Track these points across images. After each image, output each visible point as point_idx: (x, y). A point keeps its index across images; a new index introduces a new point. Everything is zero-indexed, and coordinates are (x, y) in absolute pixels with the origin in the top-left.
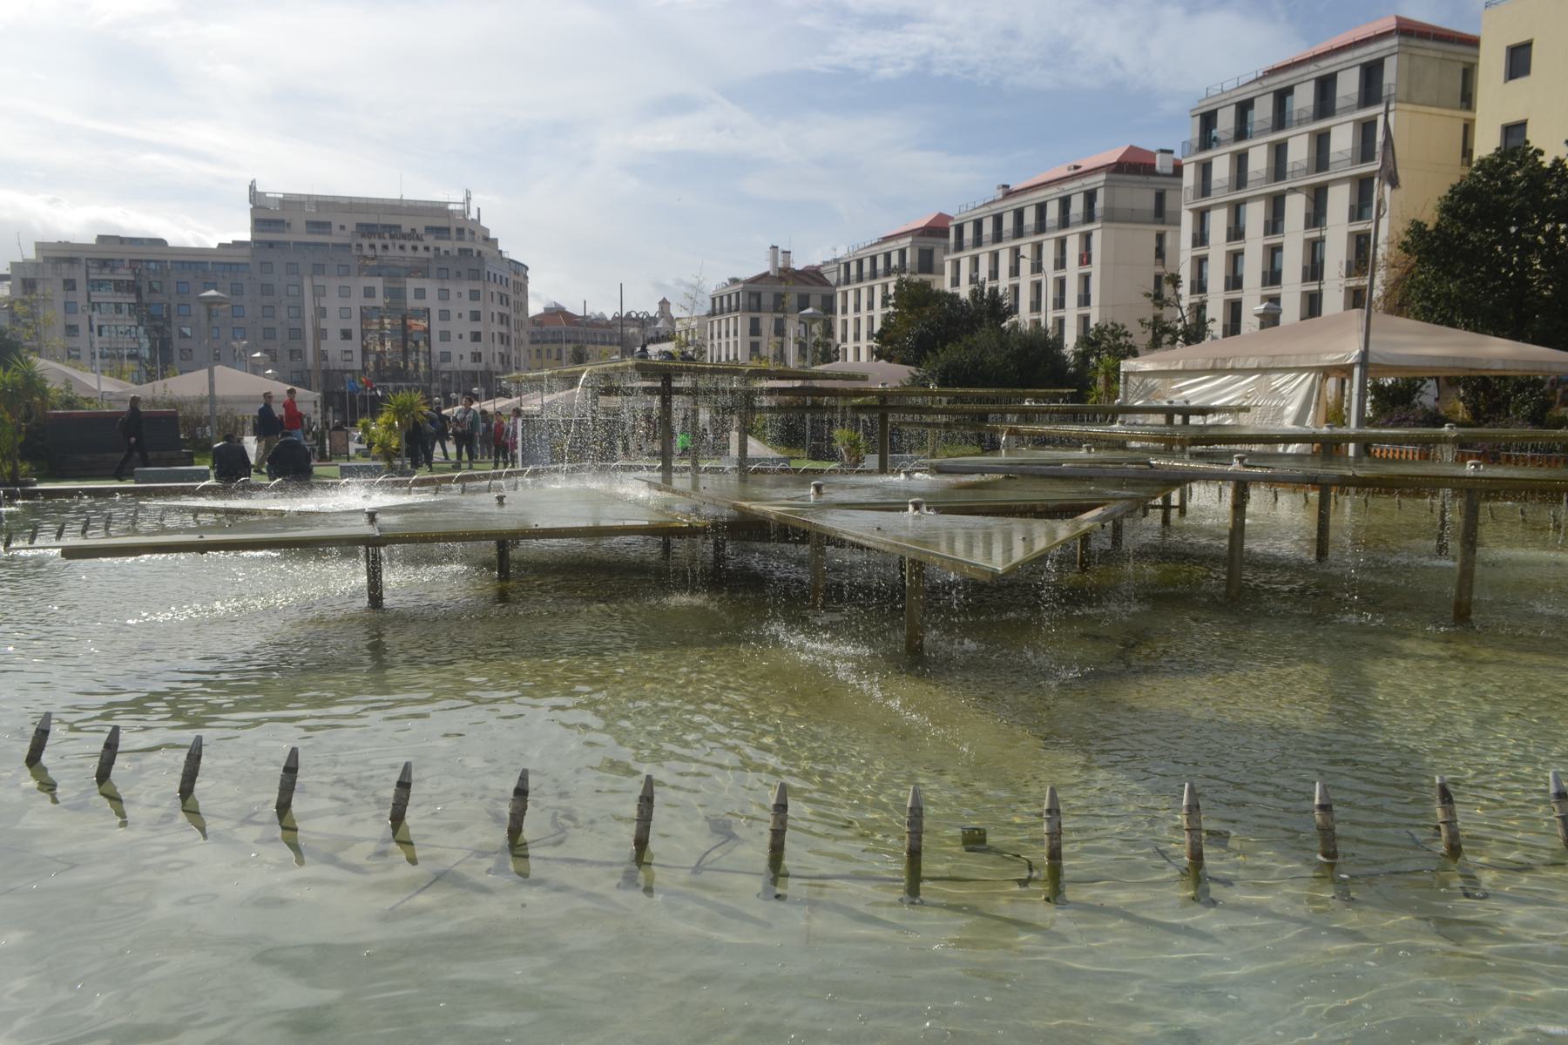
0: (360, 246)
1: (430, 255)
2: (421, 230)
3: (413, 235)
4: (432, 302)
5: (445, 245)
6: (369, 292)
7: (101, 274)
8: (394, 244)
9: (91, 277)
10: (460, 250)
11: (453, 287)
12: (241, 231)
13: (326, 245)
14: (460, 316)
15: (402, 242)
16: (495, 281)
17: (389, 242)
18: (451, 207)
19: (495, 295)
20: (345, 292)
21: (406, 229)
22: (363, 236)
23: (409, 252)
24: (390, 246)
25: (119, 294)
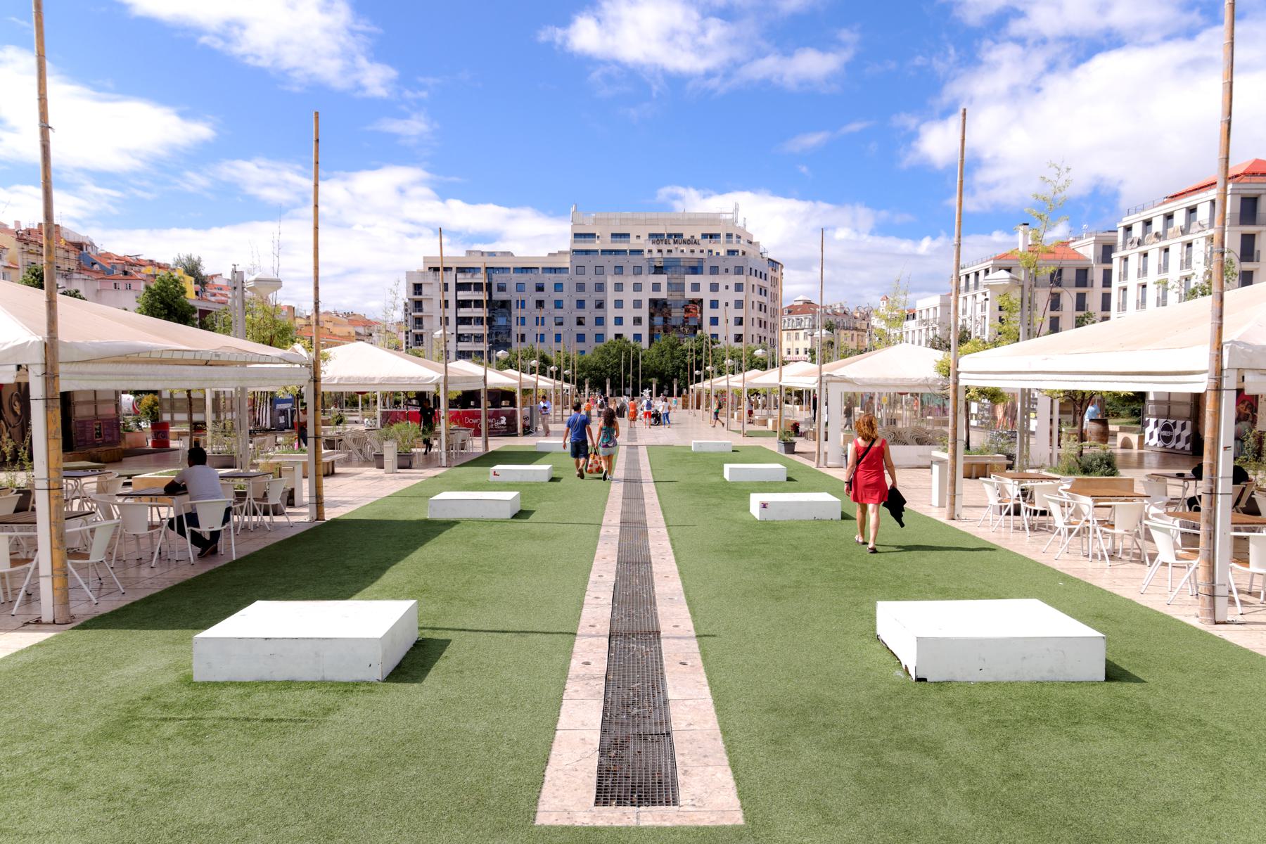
0: (650, 251)
2: (698, 237)
3: (693, 241)
4: (705, 295)
6: (656, 287)
12: (566, 245)
13: (625, 251)
18: (724, 216)
20: (637, 287)
21: (687, 236)
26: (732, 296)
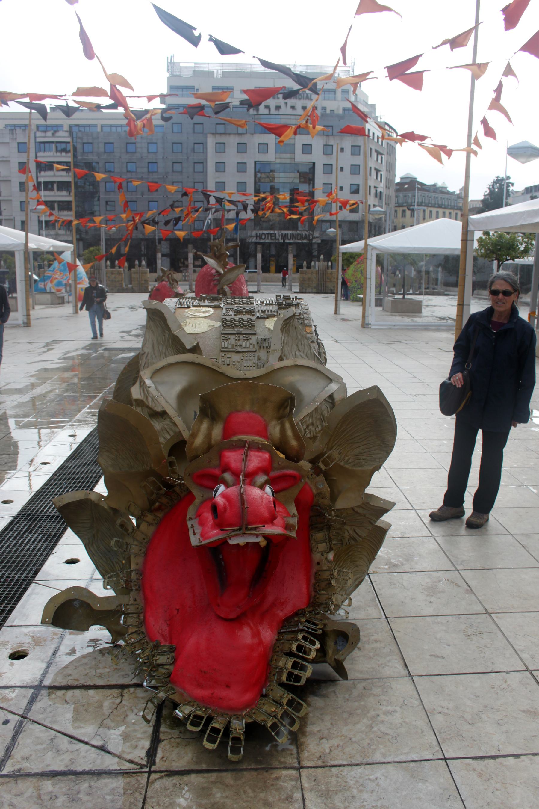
7: (45, 137)
8: (286, 104)
9: (39, 140)
19: (373, 151)
20: (242, 148)
24: (283, 106)
25: (59, 154)
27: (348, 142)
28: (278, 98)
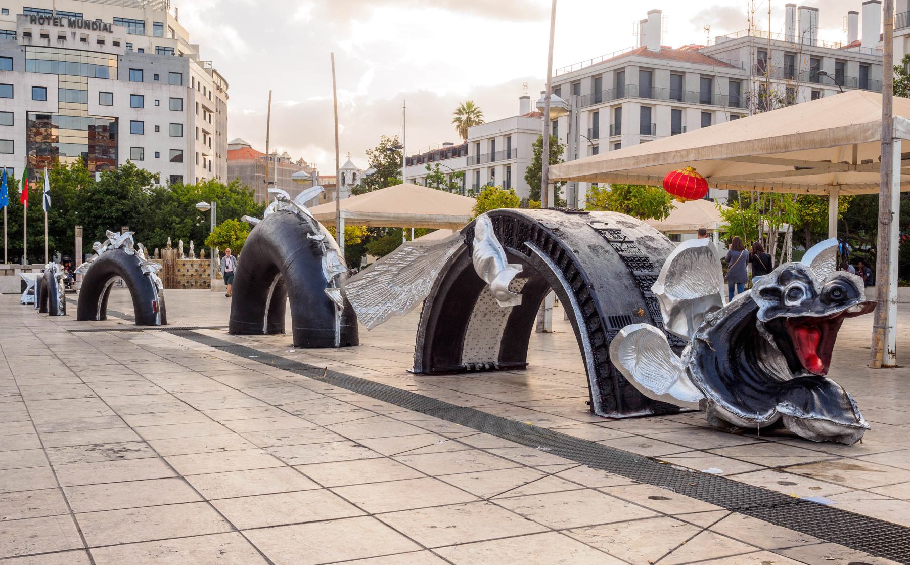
0: (28, 35)
1: (121, 50)
5: (139, 42)
10: (158, 49)
11: (149, 92)
14: (157, 129)
15: (85, 32)
16: (199, 90)
17: (67, 31)
22: (33, 20)
23: (94, 46)
26: (165, 117)
27: (165, 92)
28: (62, 26)
